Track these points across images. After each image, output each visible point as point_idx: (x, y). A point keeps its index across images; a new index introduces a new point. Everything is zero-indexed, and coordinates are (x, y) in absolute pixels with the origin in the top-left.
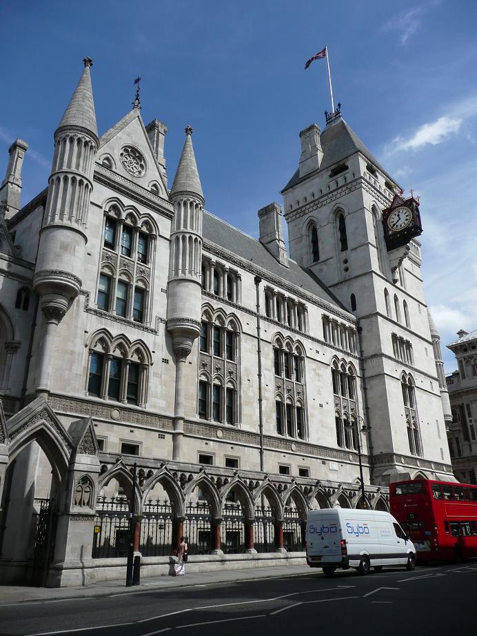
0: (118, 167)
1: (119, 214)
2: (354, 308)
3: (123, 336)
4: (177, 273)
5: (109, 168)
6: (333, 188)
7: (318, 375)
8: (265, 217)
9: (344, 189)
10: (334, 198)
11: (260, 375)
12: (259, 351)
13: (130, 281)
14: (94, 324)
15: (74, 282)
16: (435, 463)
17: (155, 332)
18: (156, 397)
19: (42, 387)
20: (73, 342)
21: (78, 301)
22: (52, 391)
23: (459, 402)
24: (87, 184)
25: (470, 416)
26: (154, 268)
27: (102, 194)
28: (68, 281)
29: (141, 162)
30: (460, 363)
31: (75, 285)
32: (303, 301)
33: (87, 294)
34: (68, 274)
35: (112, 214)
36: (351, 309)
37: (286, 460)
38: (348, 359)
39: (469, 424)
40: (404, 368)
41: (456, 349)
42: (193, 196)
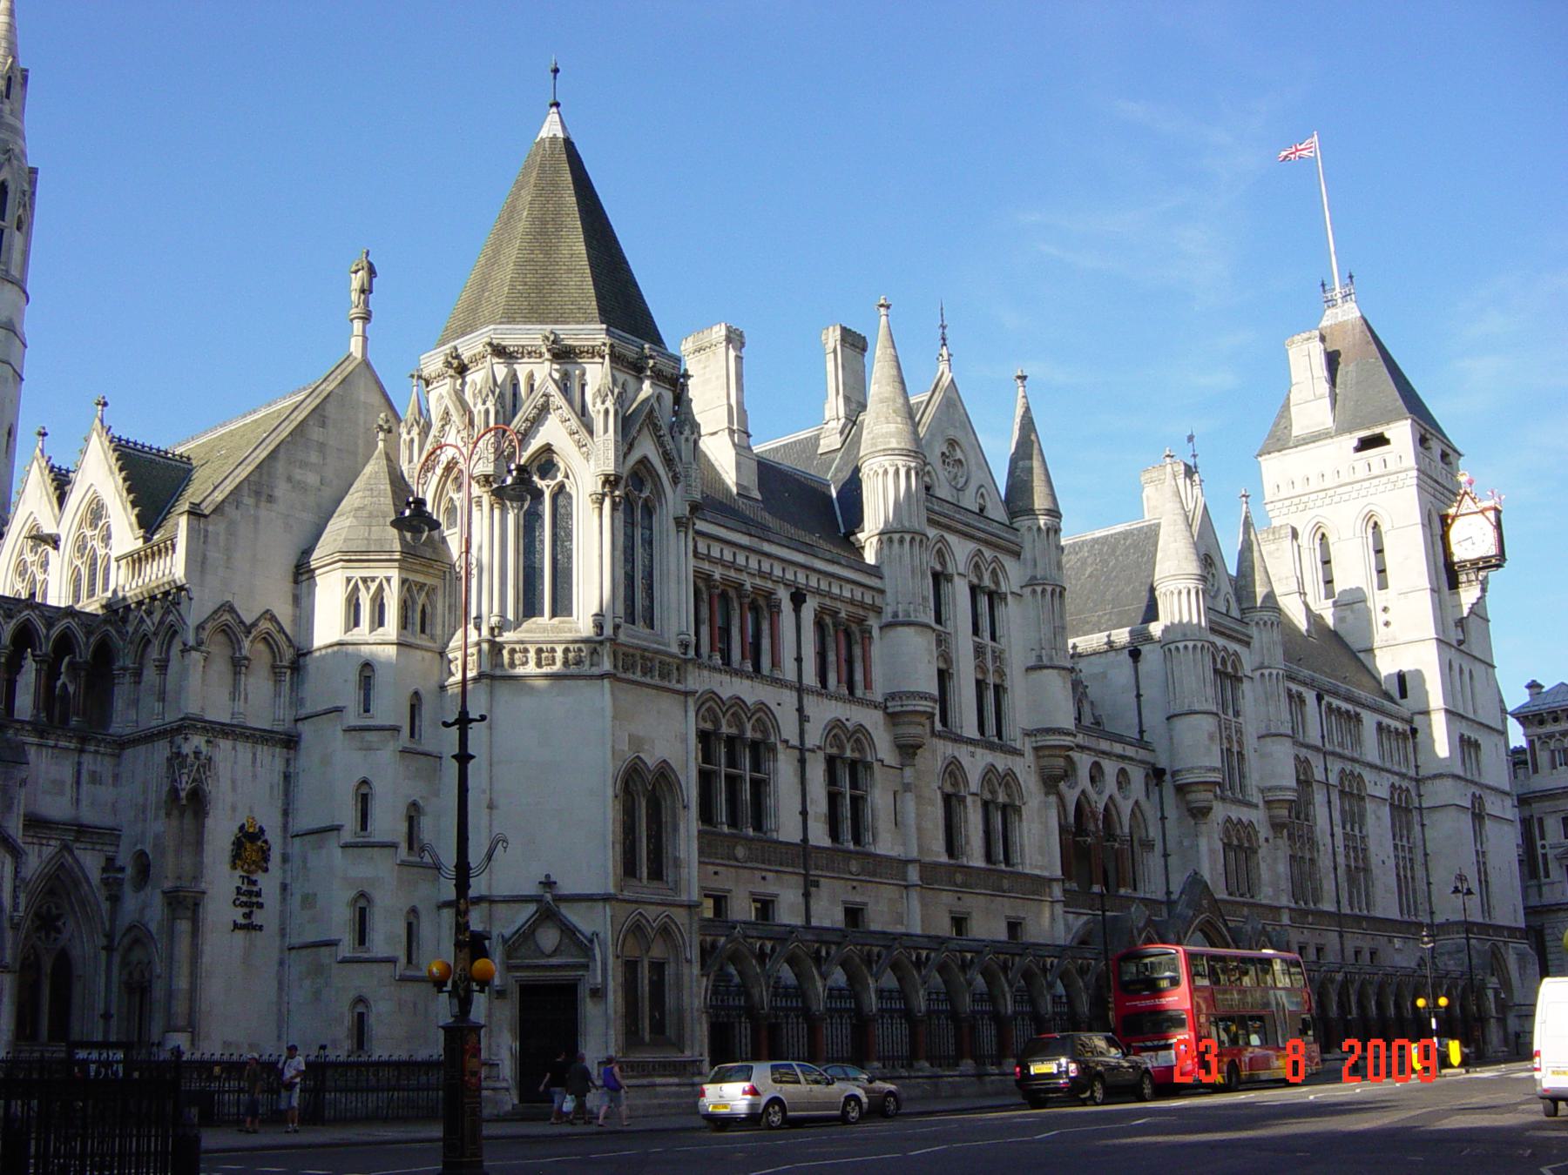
2: (1403, 694)
6: (1362, 472)
7: (1378, 818)
8: (1273, 547)
9: (1384, 480)
10: (1363, 492)
11: (1332, 835)
12: (1329, 802)
16: (1509, 928)
17: (1256, 806)
23: (1527, 814)
25: (1543, 838)
30: (1531, 743)
32: (1358, 710)
36: (1395, 693)
37: (1359, 943)
38: (1405, 784)
39: (1540, 851)
40: (1474, 789)
41: (1524, 718)
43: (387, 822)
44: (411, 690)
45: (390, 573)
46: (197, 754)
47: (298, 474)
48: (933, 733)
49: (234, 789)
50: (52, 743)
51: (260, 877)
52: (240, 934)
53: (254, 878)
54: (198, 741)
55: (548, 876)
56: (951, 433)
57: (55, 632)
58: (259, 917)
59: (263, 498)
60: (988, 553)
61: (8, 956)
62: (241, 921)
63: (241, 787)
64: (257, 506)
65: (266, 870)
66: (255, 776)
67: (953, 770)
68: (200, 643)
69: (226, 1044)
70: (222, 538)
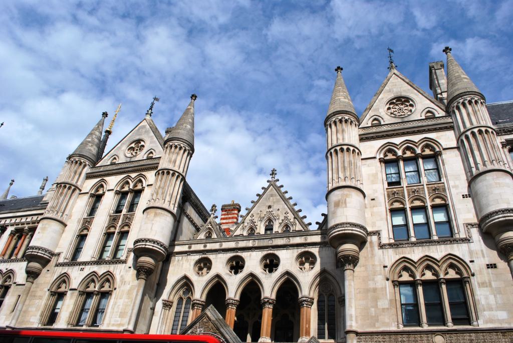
0: (387, 119)
1: (395, 153)
3: (428, 258)
4: (471, 171)
5: (380, 125)
13: (424, 203)
14: (391, 256)
15: (351, 228)
17: (467, 240)
18: (491, 309)
19: (348, 328)
20: (373, 280)
21: (371, 242)
22: (359, 330)
24: (354, 150)
26: (447, 181)
27: (372, 148)
28: (345, 230)
29: (409, 102)
31: (352, 230)
33: (377, 233)
34: (343, 224)
35: (390, 156)
42: (461, 97)
48: (57, 265)
56: (137, 138)
60: (133, 175)
67: (64, 279)
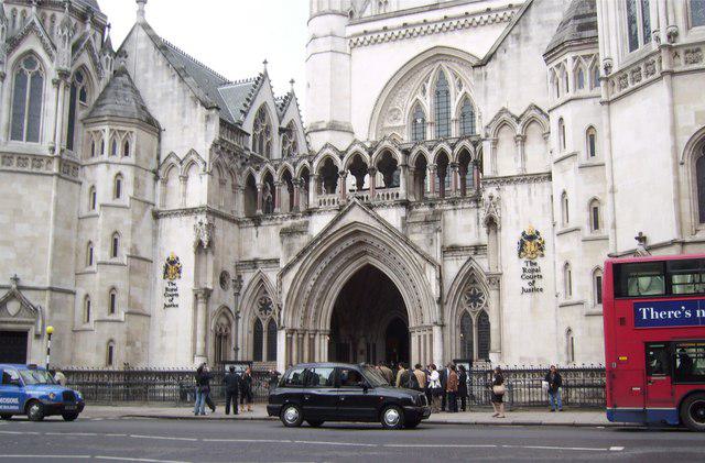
43: (579, 216)
44: (586, 126)
45: (566, 57)
46: (491, 197)
47: (545, 17)
49: (517, 212)
50: (460, 206)
51: (539, 260)
52: (529, 295)
53: (535, 261)
54: (490, 190)
55: (641, 233)
57: (456, 151)
58: (537, 285)
59: (522, 40)
61: (436, 317)
62: (528, 287)
63: (520, 210)
64: (519, 46)
65: (542, 256)
66: (531, 202)
68: (487, 136)
69: (521, 359)
70: (497, 75)
